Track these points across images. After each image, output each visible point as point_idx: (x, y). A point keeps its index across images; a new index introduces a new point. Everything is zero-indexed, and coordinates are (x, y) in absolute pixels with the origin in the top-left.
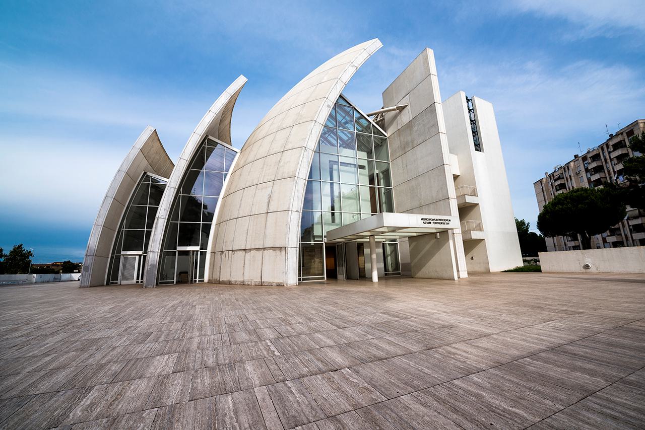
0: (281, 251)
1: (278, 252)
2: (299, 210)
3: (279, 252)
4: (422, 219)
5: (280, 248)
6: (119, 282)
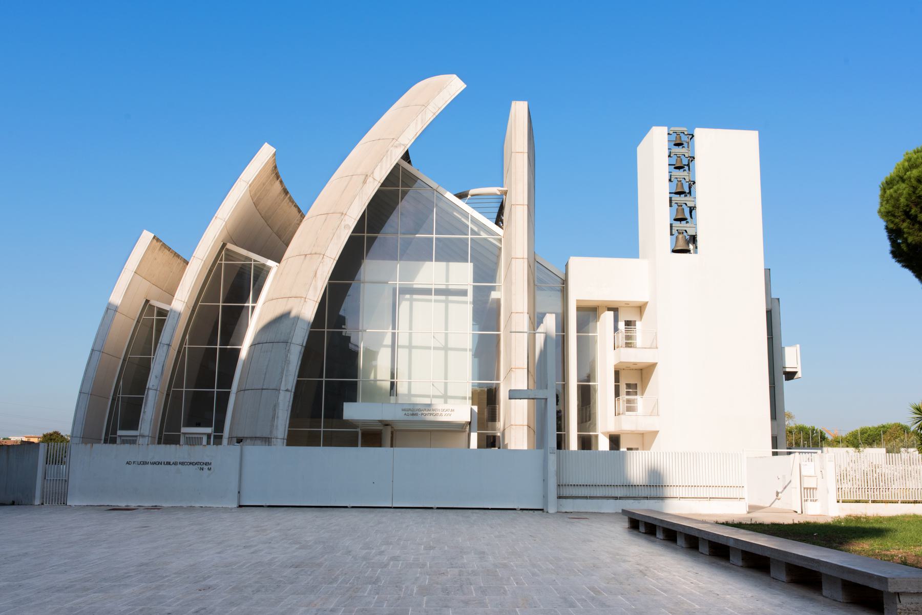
2: (290, 388)
4: (403, 410)
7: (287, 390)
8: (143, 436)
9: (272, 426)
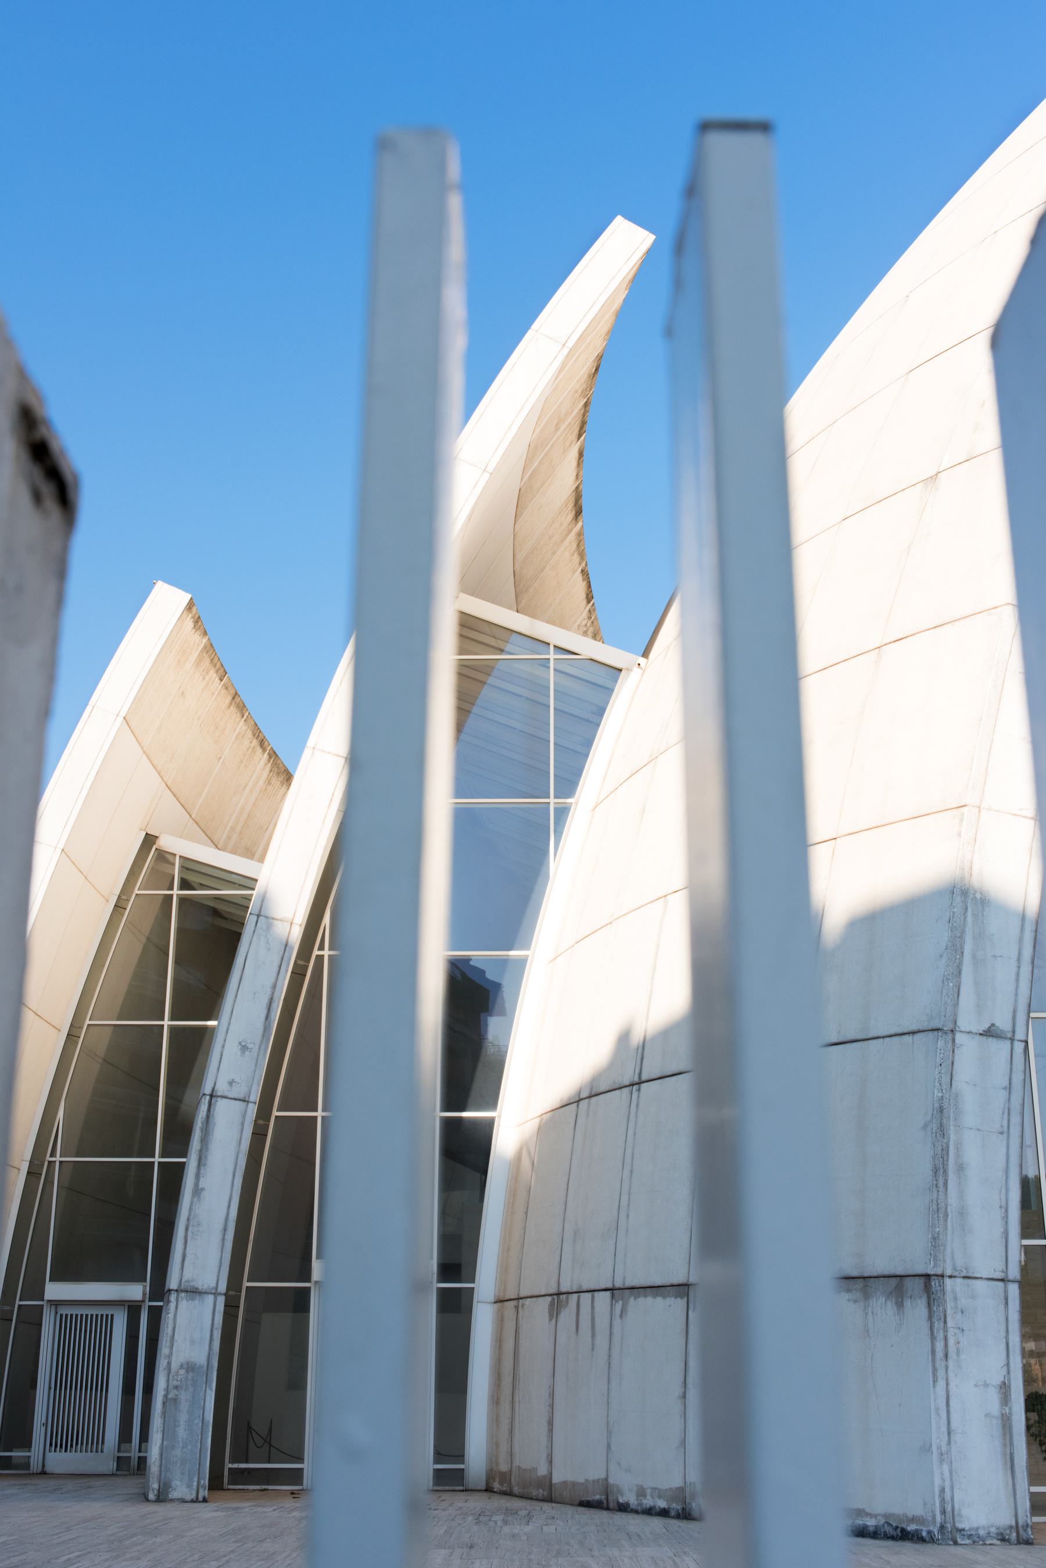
0: (900, 1305)
1: (883, 1308)
2: (1003, 1023)
3: (890, 1307)
5: (897, 1285)
6: (35, 1453)
7: (990, 1033)
8: (194, 1292)
9: (938, 1211)
